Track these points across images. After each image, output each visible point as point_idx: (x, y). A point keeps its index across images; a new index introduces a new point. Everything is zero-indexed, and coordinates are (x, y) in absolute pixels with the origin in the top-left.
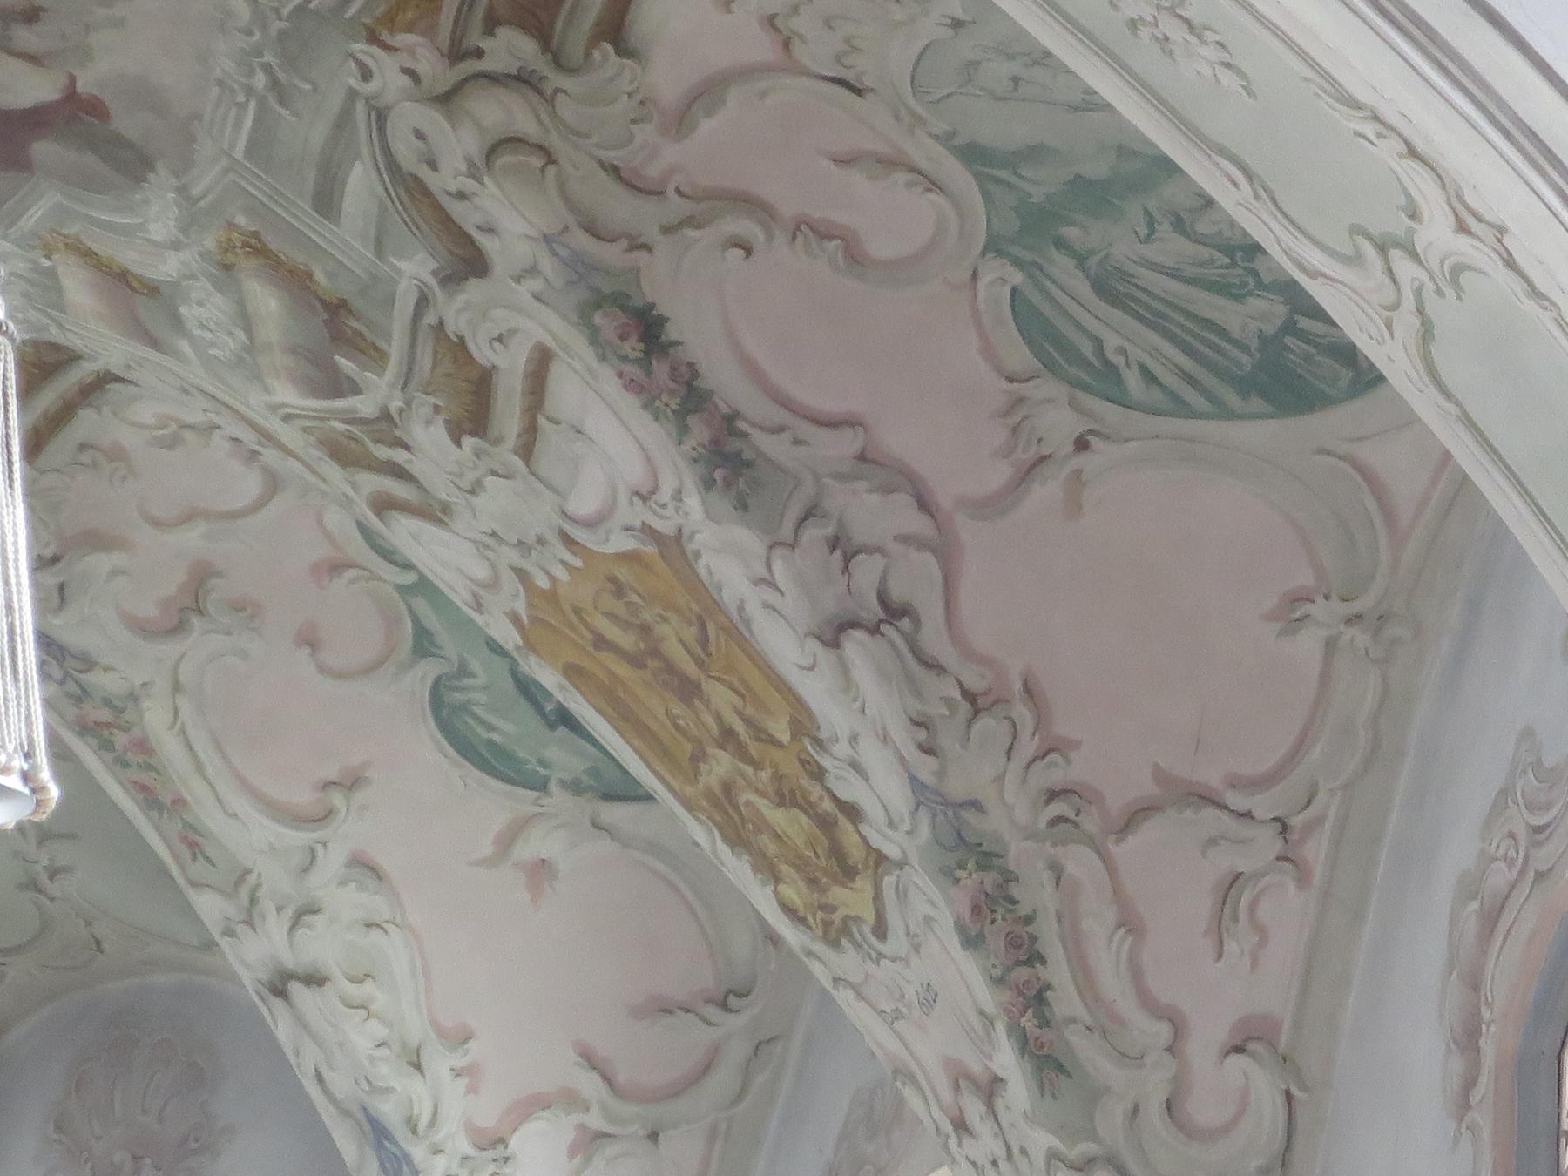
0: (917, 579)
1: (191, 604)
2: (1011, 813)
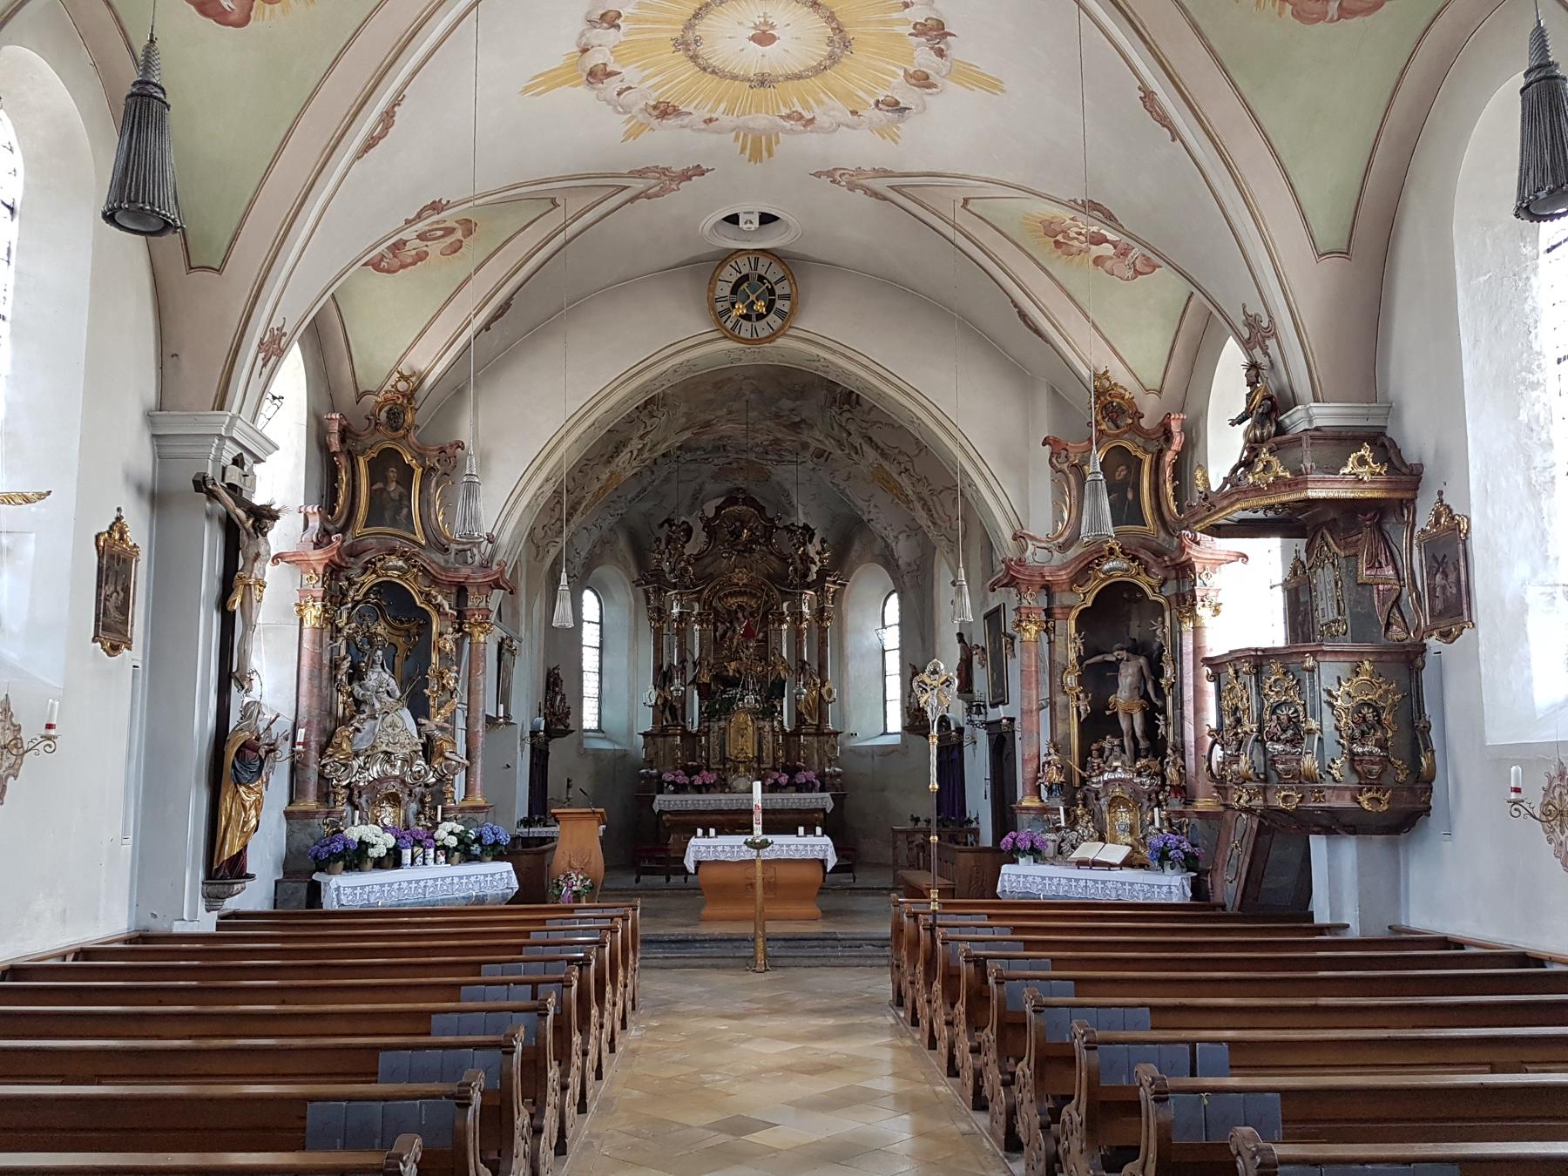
0: (909, 466)
1: (849, 478)
2: (925, 493)
